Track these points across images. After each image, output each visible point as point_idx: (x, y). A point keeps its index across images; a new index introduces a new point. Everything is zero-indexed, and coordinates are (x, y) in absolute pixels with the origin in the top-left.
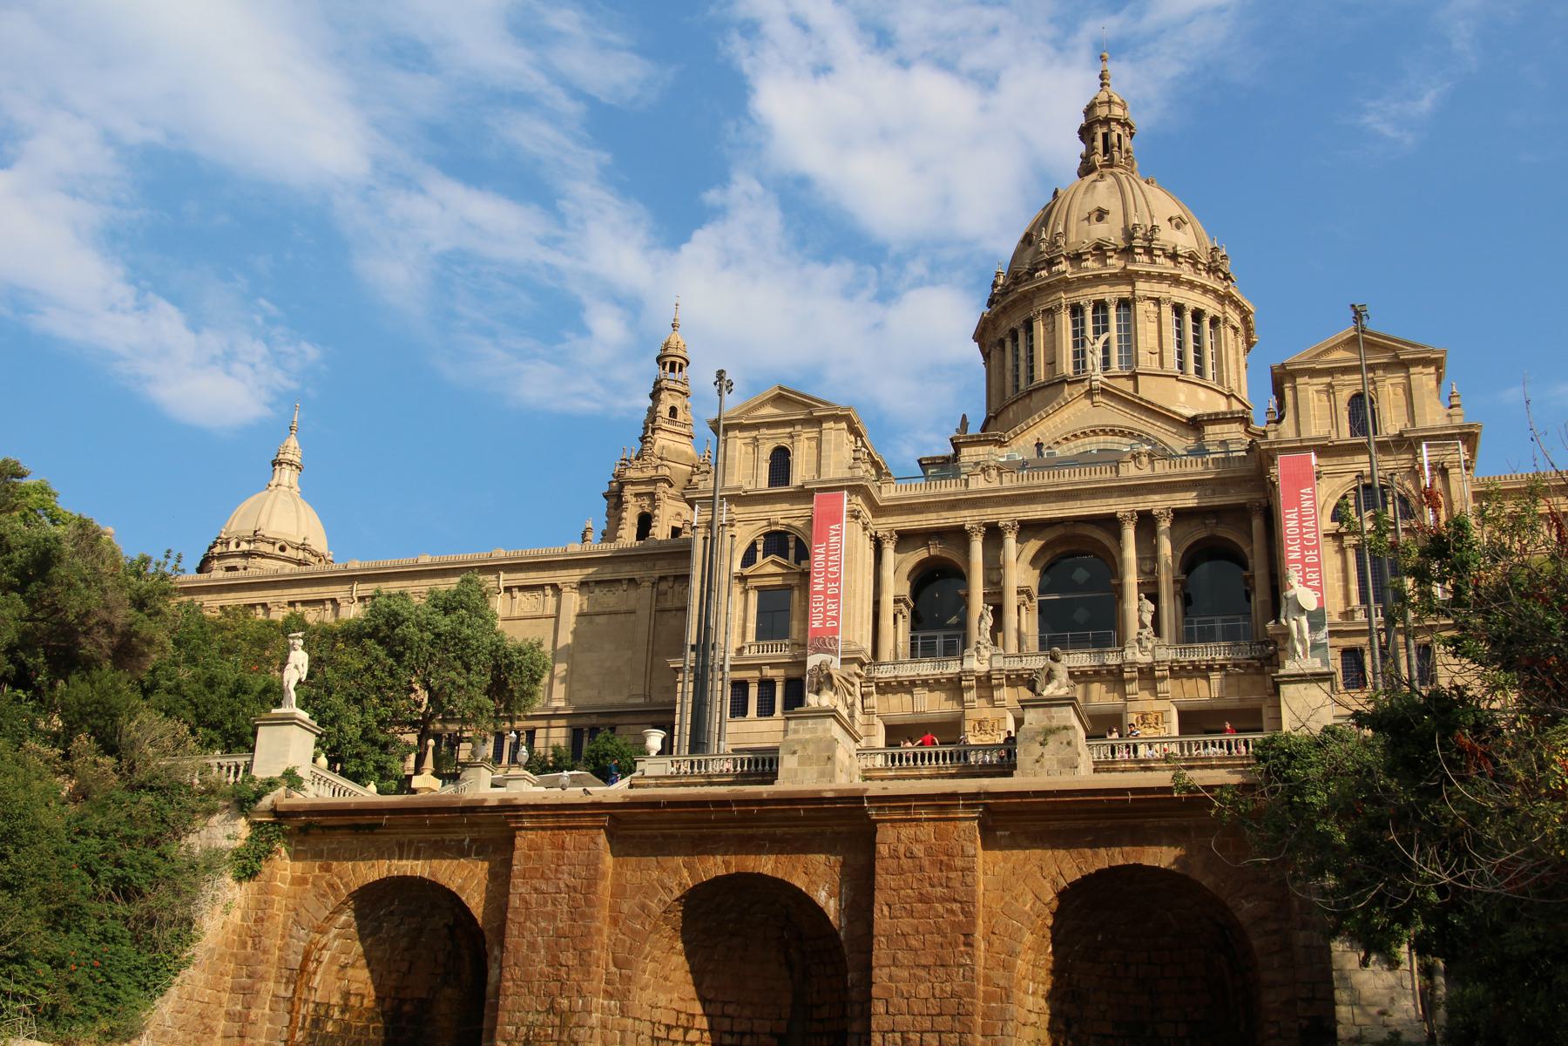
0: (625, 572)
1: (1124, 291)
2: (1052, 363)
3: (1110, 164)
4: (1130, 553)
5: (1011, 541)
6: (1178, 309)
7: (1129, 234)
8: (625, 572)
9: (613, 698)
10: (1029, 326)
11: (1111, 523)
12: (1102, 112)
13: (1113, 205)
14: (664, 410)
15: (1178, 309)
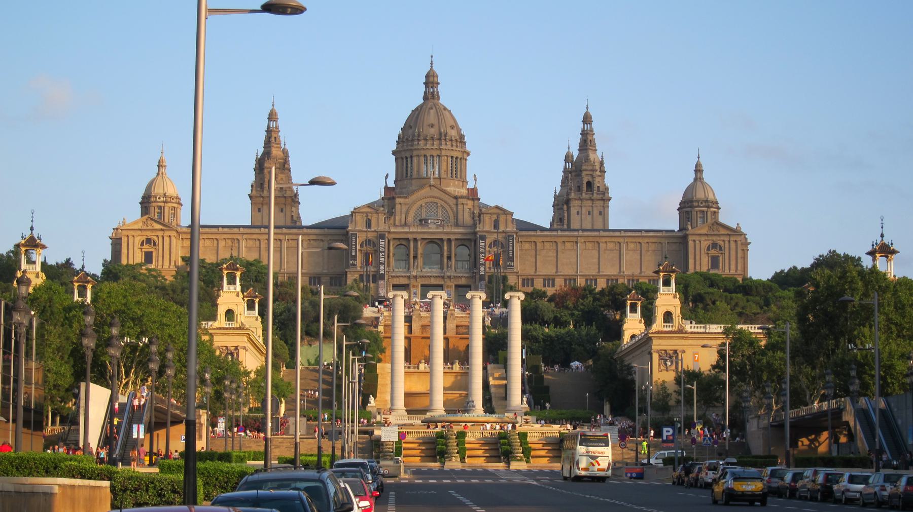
0: (320, 237)
1: (438, 152)
2: (418, 171)
3: (433, 98)
4: (445, 248)
5: (419, 243)
6: (452, 157)
7: (440, 134)
8: (320, 237)
9: (318, 270)
10: (411, 157)
11: (441, 240)
12: (431, 79)
13: (435, 122)
14: (273, 139)
15: (452, 157)
